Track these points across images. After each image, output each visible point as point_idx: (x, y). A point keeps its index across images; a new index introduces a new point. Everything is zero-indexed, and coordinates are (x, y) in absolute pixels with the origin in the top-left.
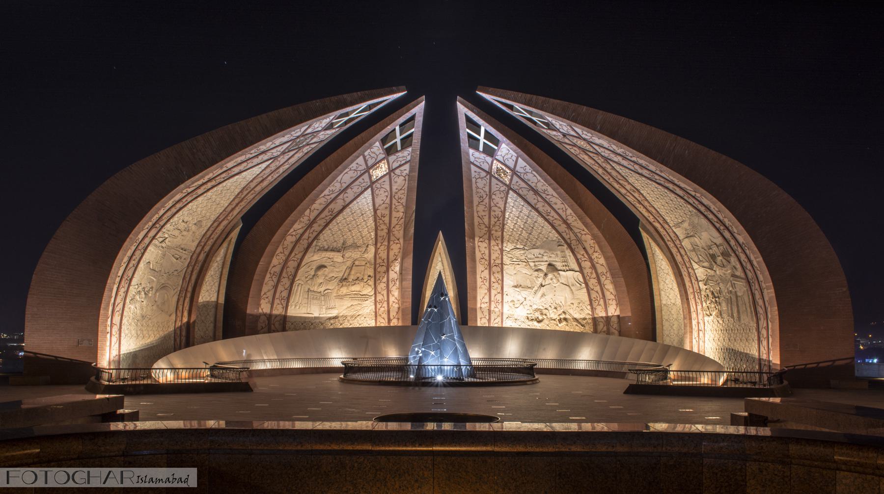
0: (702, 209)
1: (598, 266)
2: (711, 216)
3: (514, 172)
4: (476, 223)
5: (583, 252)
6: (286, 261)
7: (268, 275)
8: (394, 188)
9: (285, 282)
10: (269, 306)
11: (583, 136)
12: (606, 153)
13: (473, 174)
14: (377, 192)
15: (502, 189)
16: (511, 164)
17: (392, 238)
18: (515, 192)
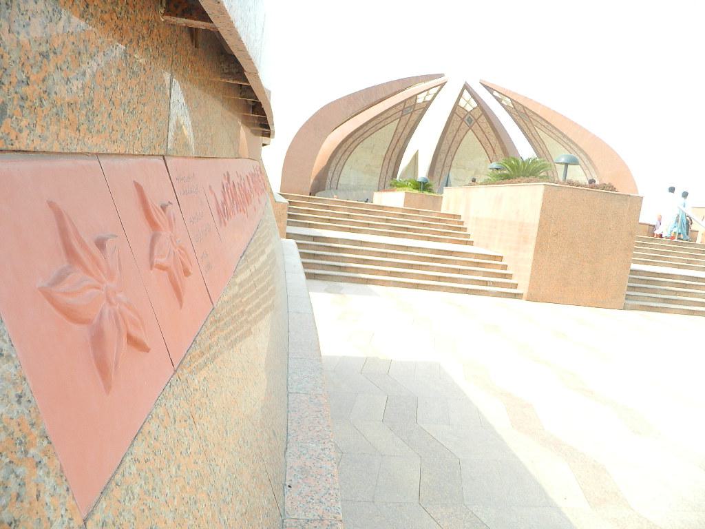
3: (476, 121)
4: (444, 143)
6: (345, 151)
9: (342, 162)
12: (535, 123)
17: (398, 145)
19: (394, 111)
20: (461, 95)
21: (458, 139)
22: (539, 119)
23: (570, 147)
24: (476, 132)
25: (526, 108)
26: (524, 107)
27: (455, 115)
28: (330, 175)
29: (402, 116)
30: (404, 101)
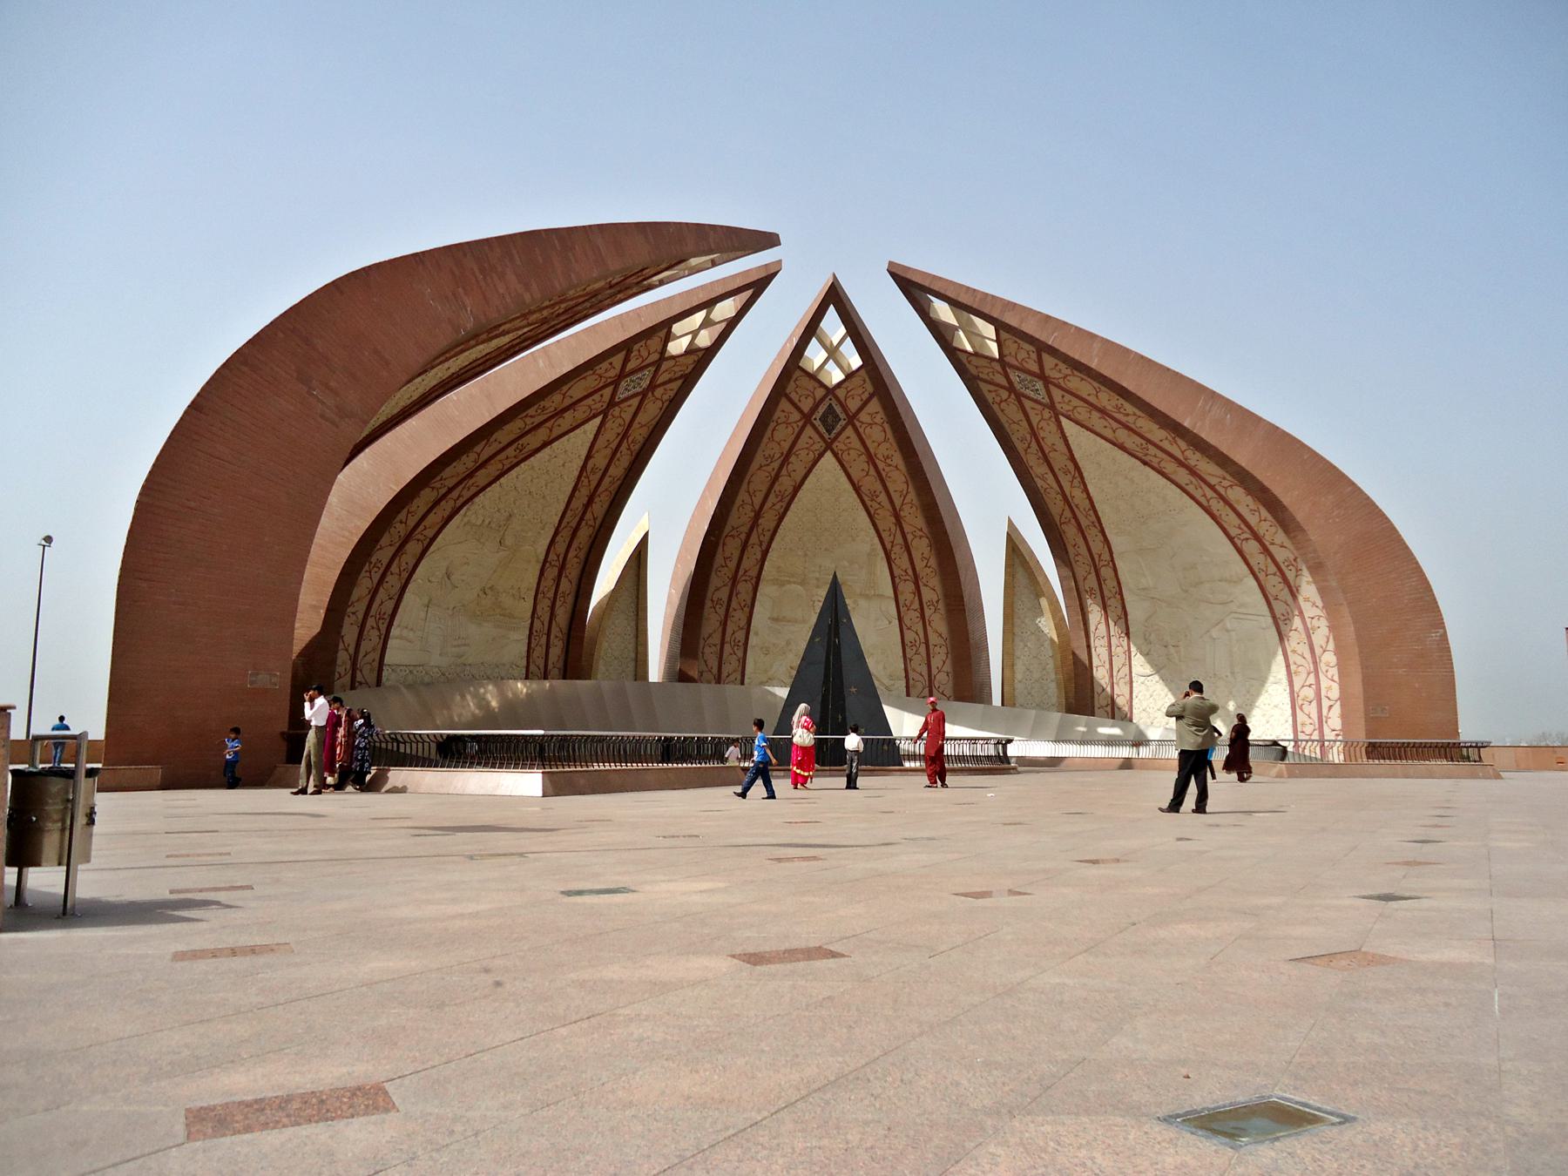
0: (1217, 506)
1: (924, 590)
2: (1231, 520)
3: (852, 419)
4: (738, 502)
5: (905, 563)
7: (366, 567)
8: (638, 419)
9: (393, 582)
10: (356, 630)
11: (1048, 372)
13: (778, 414)
14: (608, 425)
15: (817, 447)
16: (853, 405)
17: (588, 516)
18: (835, 455)
19: (590, 382)
20: (812, 329)
21: (785, 483)
22: (1085, 388)
23: (1193, 472)
24: (845, 457)
25: (1053, 351)
26: (1042, 348)
27: (784, 404)
28: (349, 632)
29: (612, 404)
30: (626, 346)
